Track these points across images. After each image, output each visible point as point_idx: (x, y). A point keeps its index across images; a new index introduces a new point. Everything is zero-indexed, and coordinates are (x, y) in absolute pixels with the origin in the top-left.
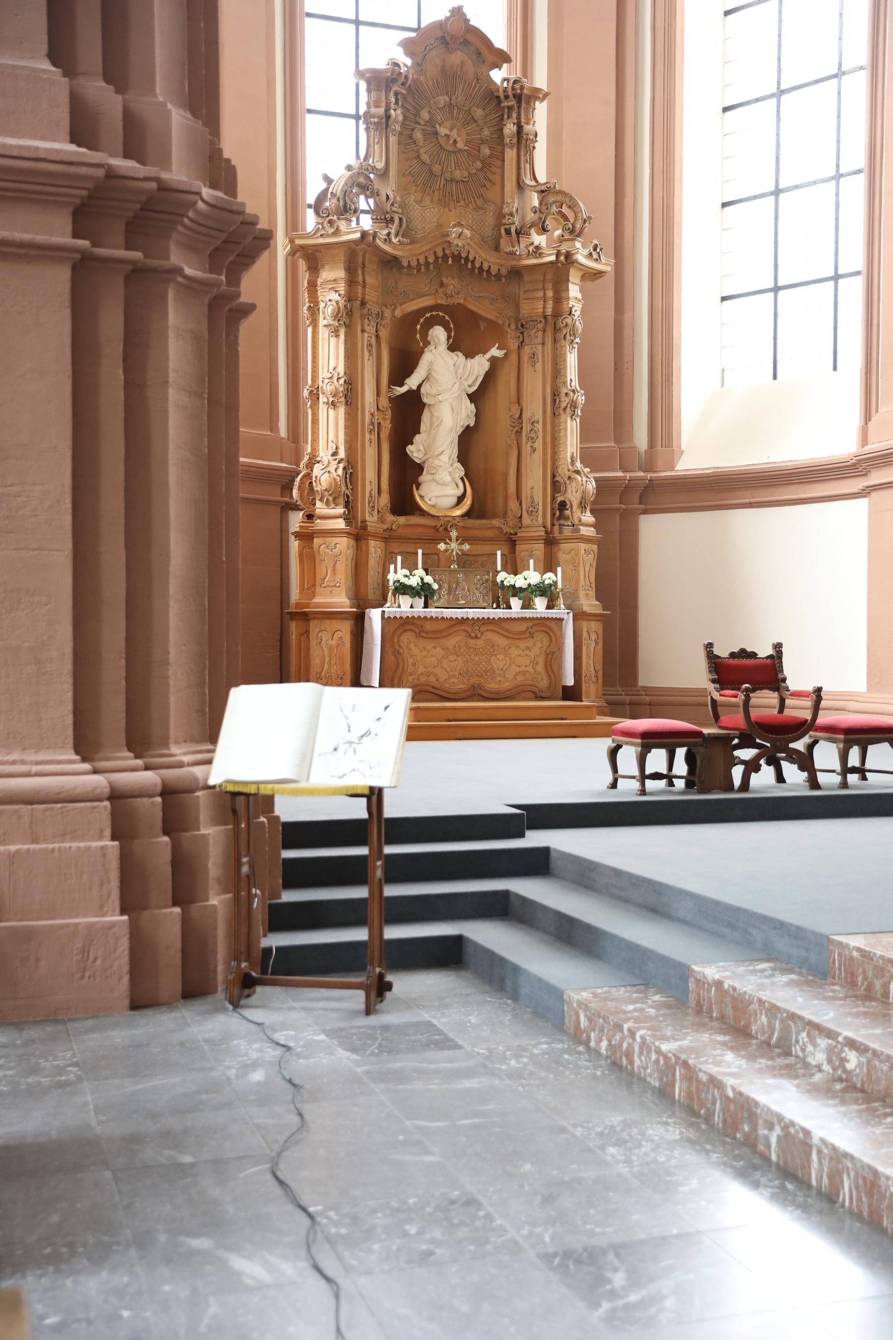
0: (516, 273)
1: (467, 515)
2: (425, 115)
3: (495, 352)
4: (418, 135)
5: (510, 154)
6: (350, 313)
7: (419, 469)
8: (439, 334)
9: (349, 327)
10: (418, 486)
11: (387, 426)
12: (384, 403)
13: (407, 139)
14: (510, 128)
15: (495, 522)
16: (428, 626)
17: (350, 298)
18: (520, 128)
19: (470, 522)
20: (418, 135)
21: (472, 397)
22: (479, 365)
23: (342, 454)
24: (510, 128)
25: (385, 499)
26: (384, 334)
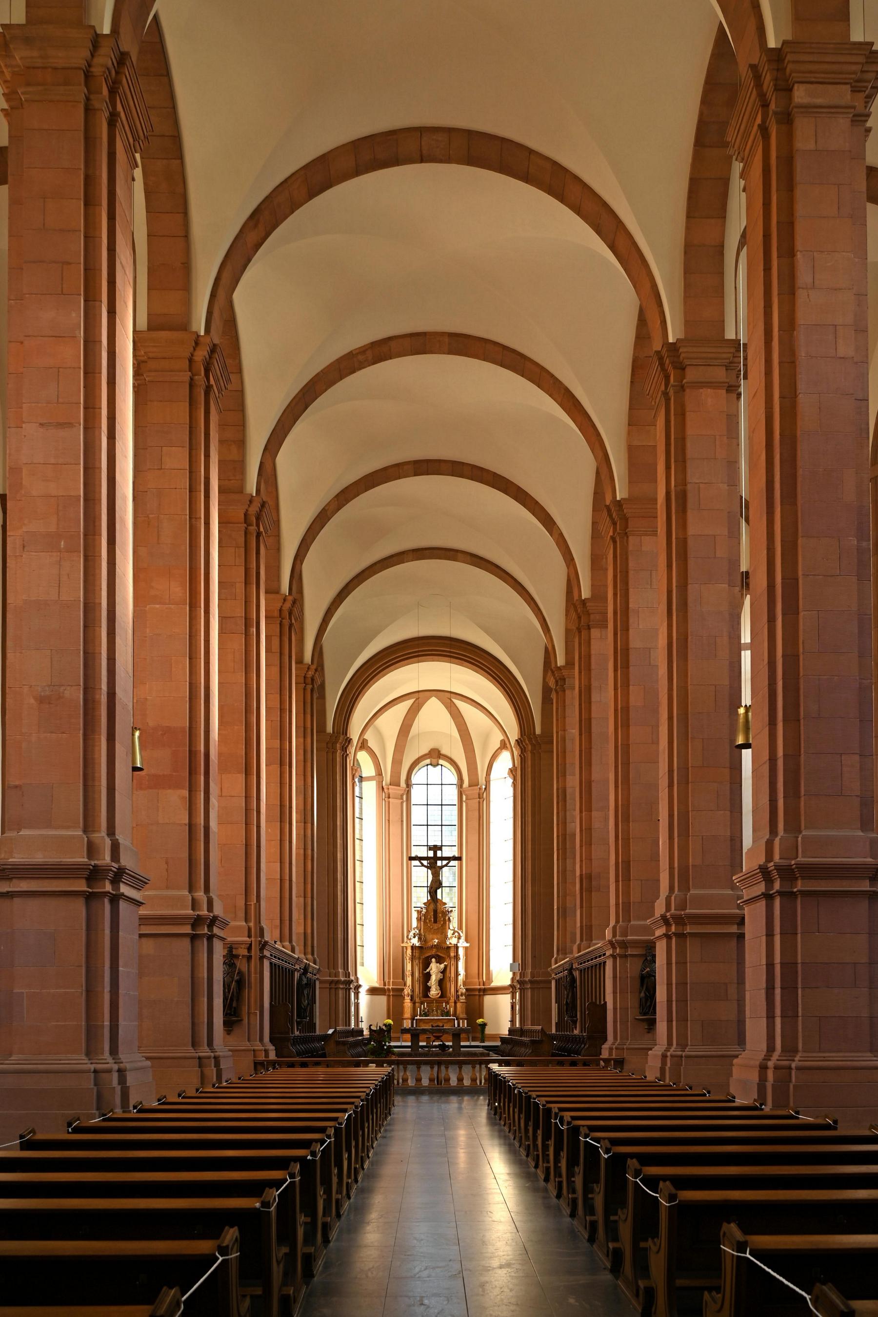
0: (449, 948)
1: (440, 997)
2: (429, 917)
3: (445, 963)
4: (427, 921)
5: (447, 923)
6: (412, 959)
7: (430, 988)
8: (433, 960)
9: (412, 961)
10: (430, 991)
11: (421, 980)
12: (421, 975)
13: (425, 922)
14: (447, 918)
15: (445, 999)
16: (426, 1021)
17: (412, 955)
18: (449, 918)
19: (440, 999)
20: (427, 921)
21: (441, 973)
22: (442, 966)
23: (410, 987)
24: (447, 918)
25: (421, 995)
26: (421, 961)
